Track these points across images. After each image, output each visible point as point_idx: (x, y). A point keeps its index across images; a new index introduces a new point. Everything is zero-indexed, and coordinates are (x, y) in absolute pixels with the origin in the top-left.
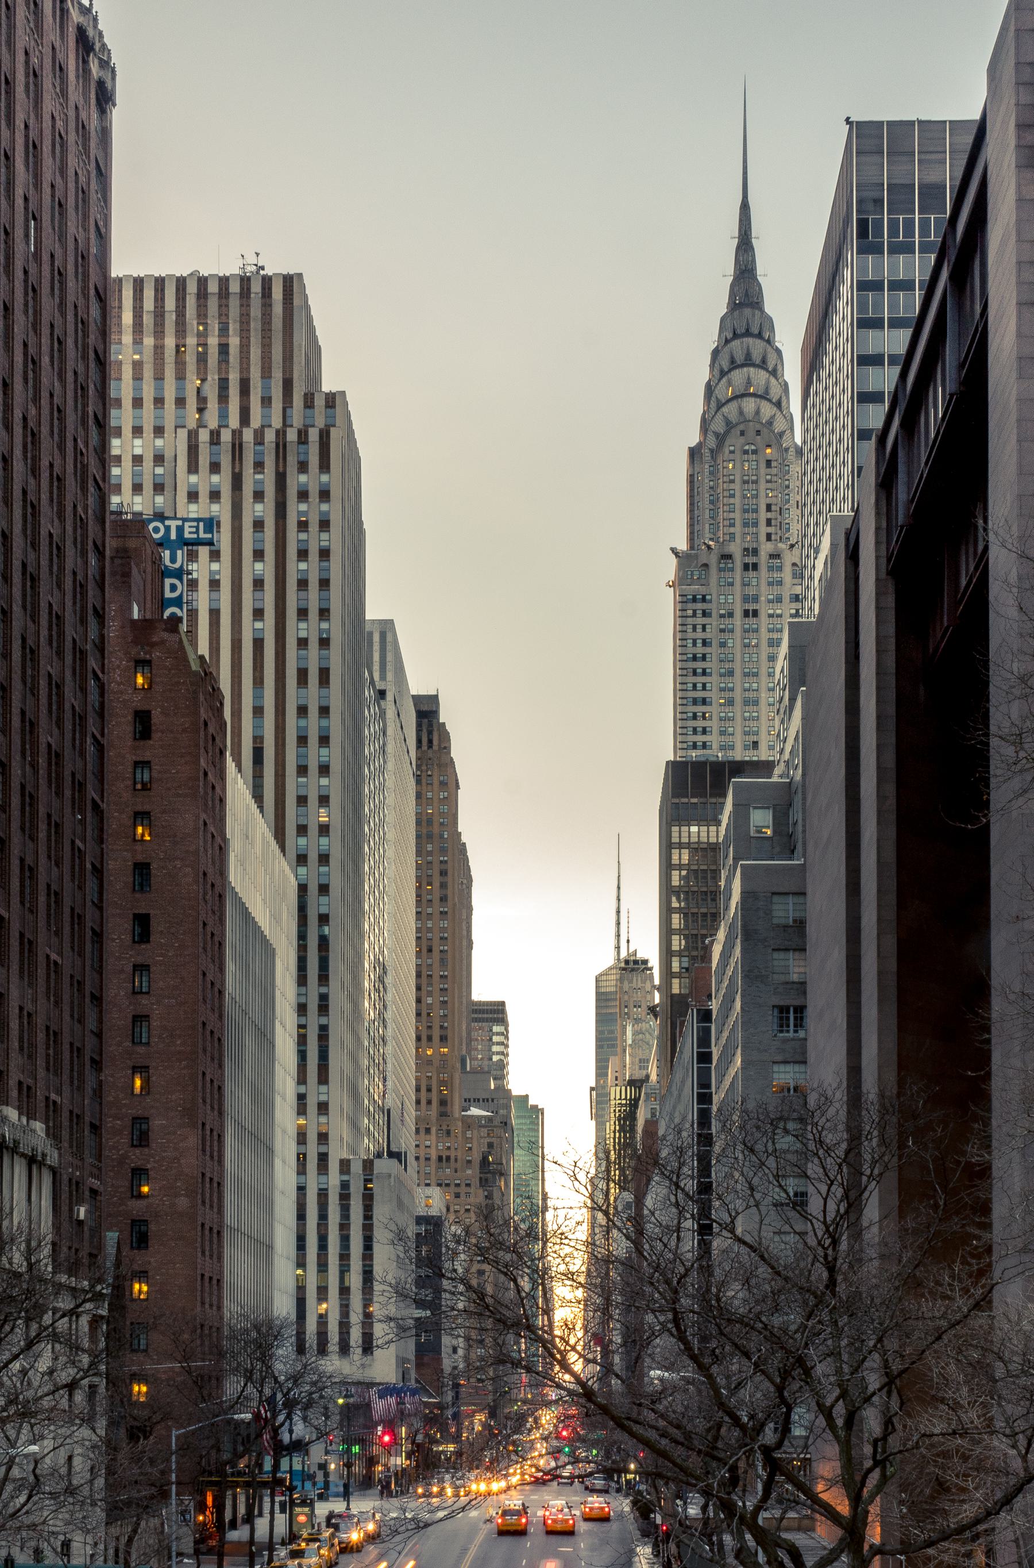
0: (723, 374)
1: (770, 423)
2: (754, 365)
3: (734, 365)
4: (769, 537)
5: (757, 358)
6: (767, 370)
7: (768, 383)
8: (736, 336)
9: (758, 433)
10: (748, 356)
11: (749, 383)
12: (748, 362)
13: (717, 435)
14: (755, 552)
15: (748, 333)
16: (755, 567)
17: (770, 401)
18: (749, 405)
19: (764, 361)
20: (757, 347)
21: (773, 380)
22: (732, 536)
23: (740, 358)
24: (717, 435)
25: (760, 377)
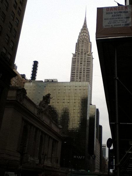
1: (86, 39)
3: (82, 33)
4: (84, 51)
5: (85, 31)
8: (83, 30)
11: (84, 34)
12: (84, 32)
13: (79, 40)
15: (84, 29)
18: (83, 37)
19: (86, 32)
20: (85, 31)
22: (80, 51)
23: (83, 32)
24: (79, 40)
25: (85, 34)
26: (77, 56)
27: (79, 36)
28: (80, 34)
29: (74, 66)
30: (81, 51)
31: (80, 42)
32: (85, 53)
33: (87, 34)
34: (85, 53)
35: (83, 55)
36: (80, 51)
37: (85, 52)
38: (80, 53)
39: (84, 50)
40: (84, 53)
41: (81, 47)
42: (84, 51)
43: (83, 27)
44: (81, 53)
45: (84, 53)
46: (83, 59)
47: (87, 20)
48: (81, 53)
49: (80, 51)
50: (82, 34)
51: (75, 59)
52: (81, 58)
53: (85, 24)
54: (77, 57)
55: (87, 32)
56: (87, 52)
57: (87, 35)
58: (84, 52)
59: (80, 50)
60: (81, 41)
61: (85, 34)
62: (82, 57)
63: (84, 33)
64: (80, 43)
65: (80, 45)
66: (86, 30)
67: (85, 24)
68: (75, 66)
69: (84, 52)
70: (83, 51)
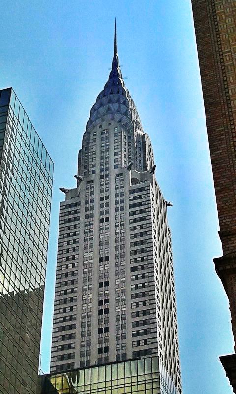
3: (101, 105)
4: (116, 167)
7: (120, 107)
11: (109, 109)
12: (110, 101)
19: (118, 101)
20: (114, 97)
22: (94, 172)
26: (82, 195)
28: (94, 110)
29: (69, 236)
30: (102, 170)
31: (92, 137)
32: (121, 174)
33: (123, 106)
36: (98, 171)
37: (117, 171)
40: (113, 177)
43: (107, 86)
47: (120, 62)
48: (102, 177)
49: (98, 171)
50: (102, 110)
51: (76, 204)
52: (102, 199)
53: (114, 75)
55: (122, 101)
58: (114, 172)
59: (94, 166)
60: (99, 133)
61: (117, 105)
62: (104, 195)
63: (110, 105)
64: (94, 140)
65: (96, 148)
66: (118, 92)
67: (114, 75)
68: (75, 234)
69: (114, 172)
70: (107, 169)
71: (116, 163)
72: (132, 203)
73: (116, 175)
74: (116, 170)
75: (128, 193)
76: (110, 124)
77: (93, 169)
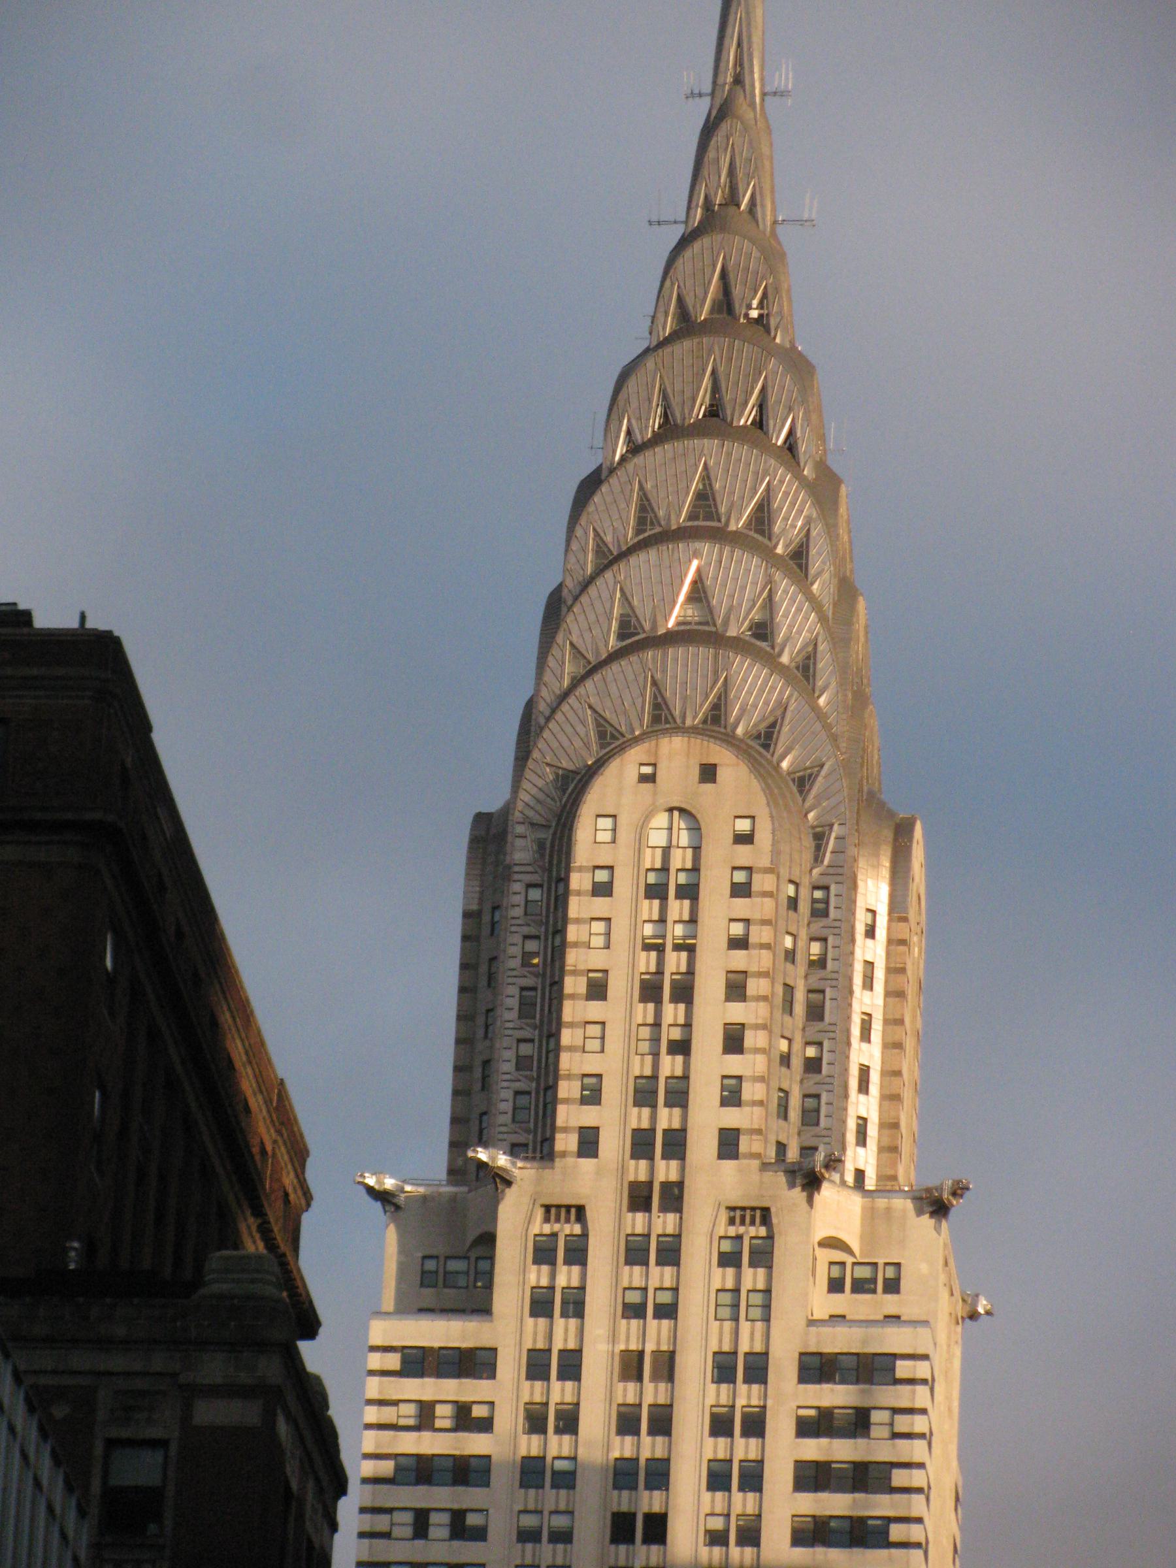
0: (609, 560)
1: (767, 737)
2: (720, 535)
4: (728, 1145)
6: (767, 554)
9: (708, 773)
10: (705, 499)
14: (674, 1196)
16: (671, 1253)
17: (771, 661)
19: (763, 518)
21: (785, 589)
22: (589, 1143)
27: (555, 609)
30: (642, 1144)
34: (738, 1213)
35: (699, 1252)
36: (613, 1144)
38: (597, 1183)
39: (707, 1117)
41: (621, 1010)
42: (702, 1145)
44: (639, 1198)
45: (703, 1228)
46: (696, 1395)
49: (613, 1144)
51: (473, 1363)
52: (631, 1366)
54: (508, 1329)
56: (812, 1183)
57: (797, 625)
58: (715, 1185)
59: (592, 1095)
70: (676, 1143)
71: (732, 1118)
72: (814, 1449)
73: (732, 1209)
74: (729, 1165)
75: (792, 1372)
76: (708, 773)
77: (588, 1116)
